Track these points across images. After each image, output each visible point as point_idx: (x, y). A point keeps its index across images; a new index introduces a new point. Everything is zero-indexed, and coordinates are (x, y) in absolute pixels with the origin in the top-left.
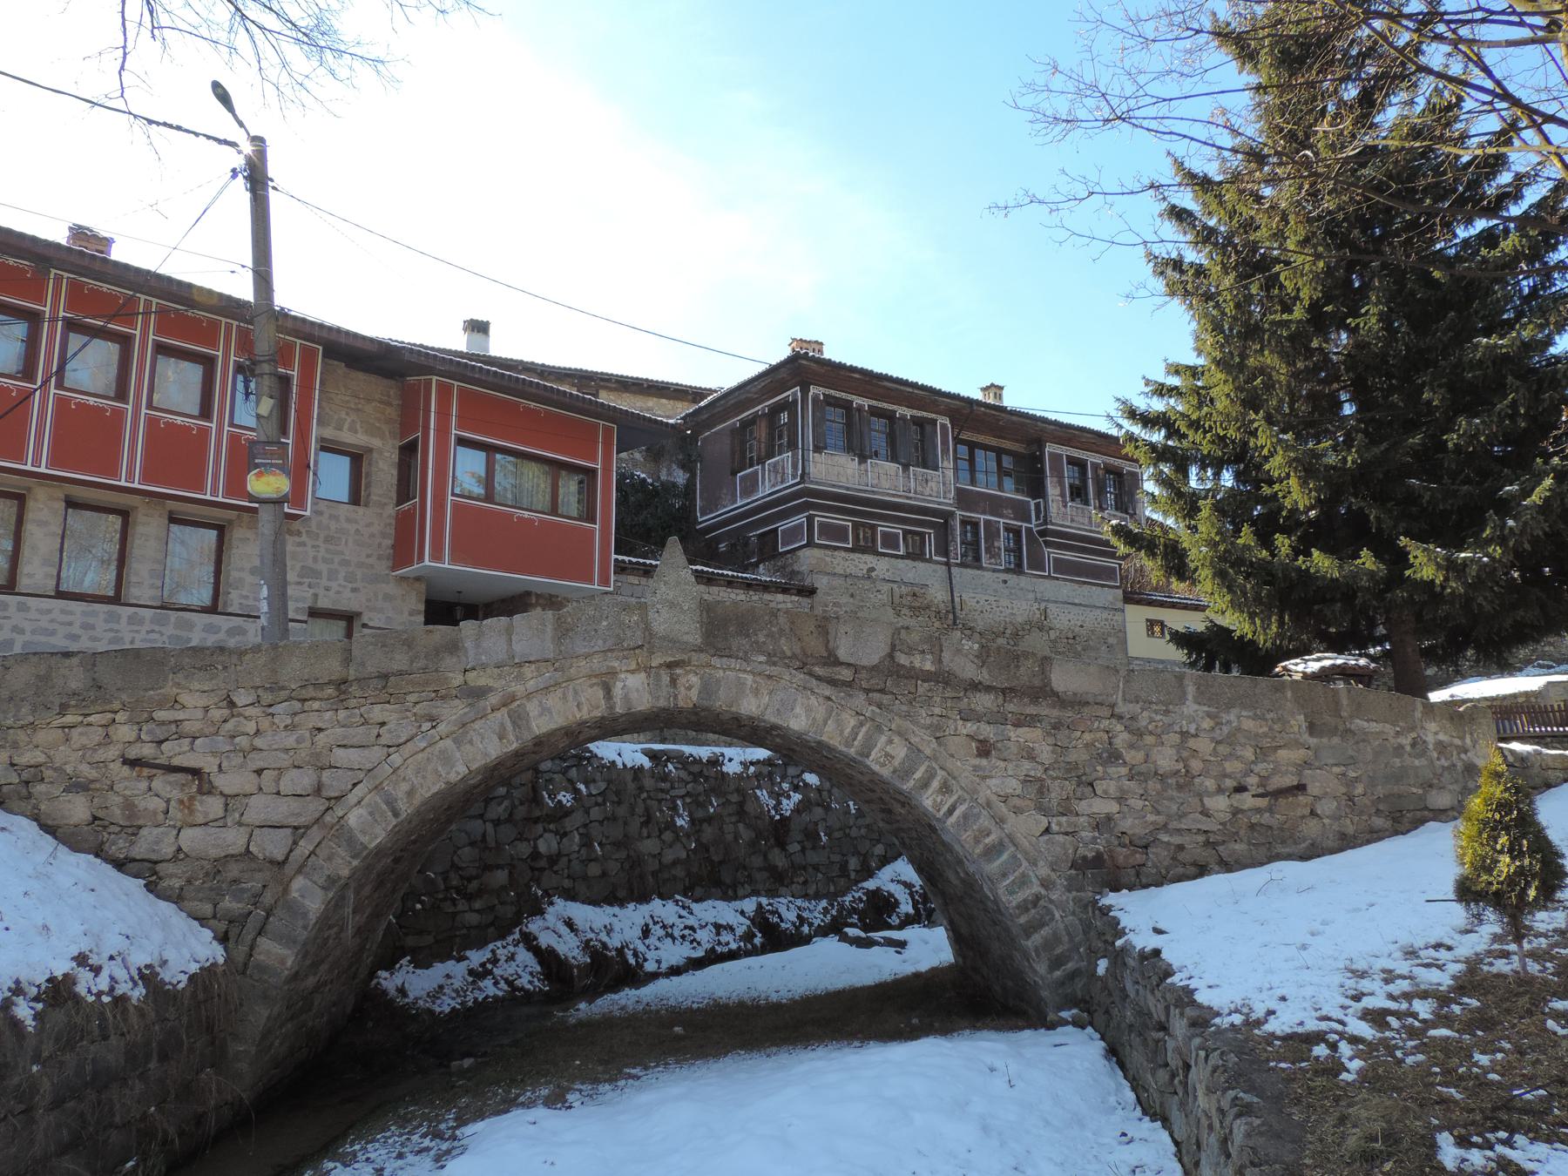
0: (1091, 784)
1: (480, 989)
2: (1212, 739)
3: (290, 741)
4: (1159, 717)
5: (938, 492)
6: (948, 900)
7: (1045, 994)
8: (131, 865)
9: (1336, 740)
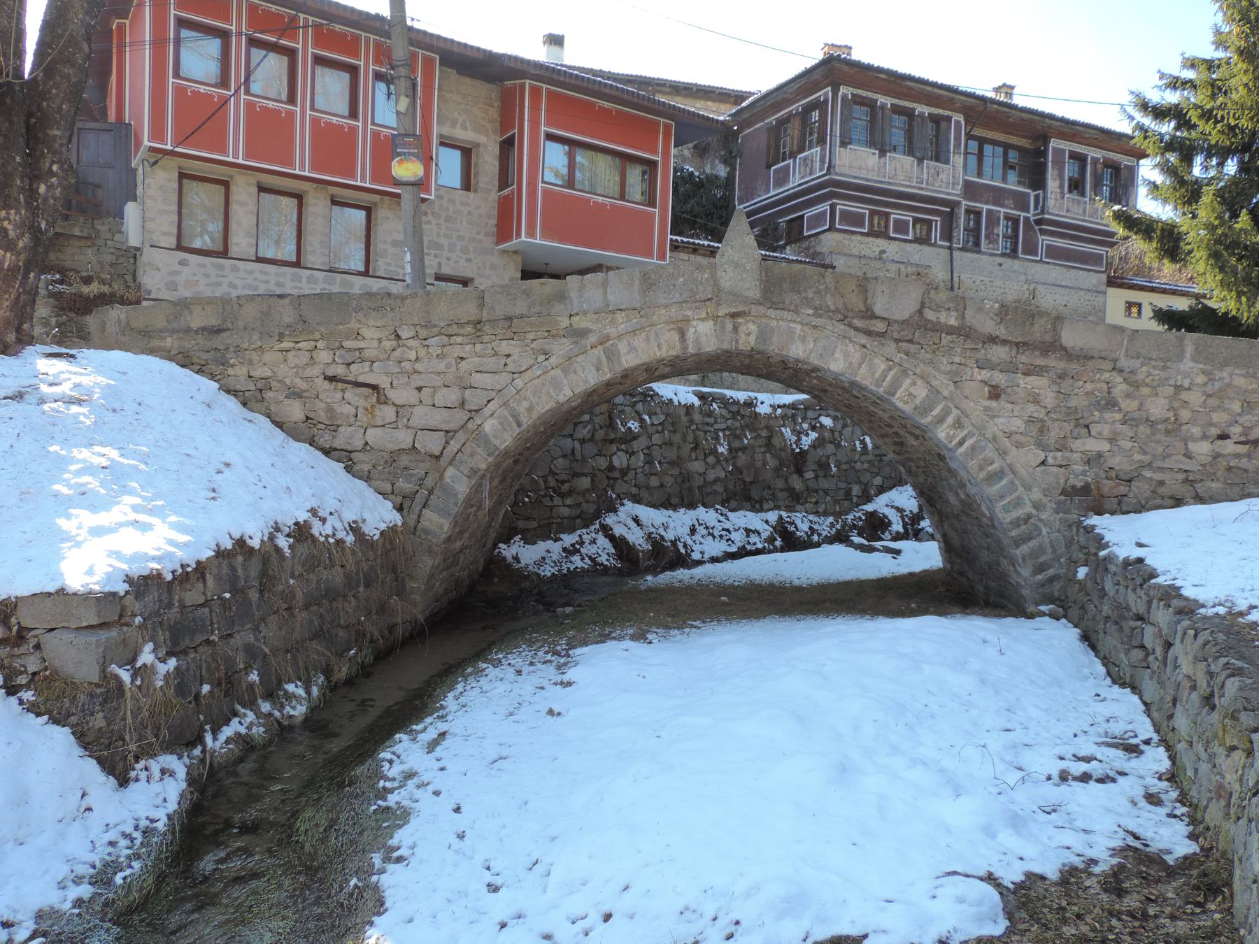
0: (1087, 427)
1: (571, 562)
2: (1204, 393)
3: (441, 366)
4: (1157, 372)
6: (941, 518)
7: (1026, 592)
8: (333, 453)
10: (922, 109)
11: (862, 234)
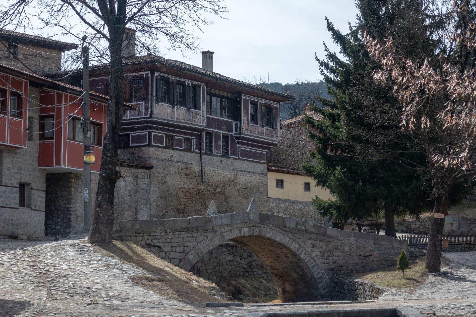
3: (178, 240)
5: (200, 121)
9: (378, 246)
10: (189, 82)
11: (163, 147)
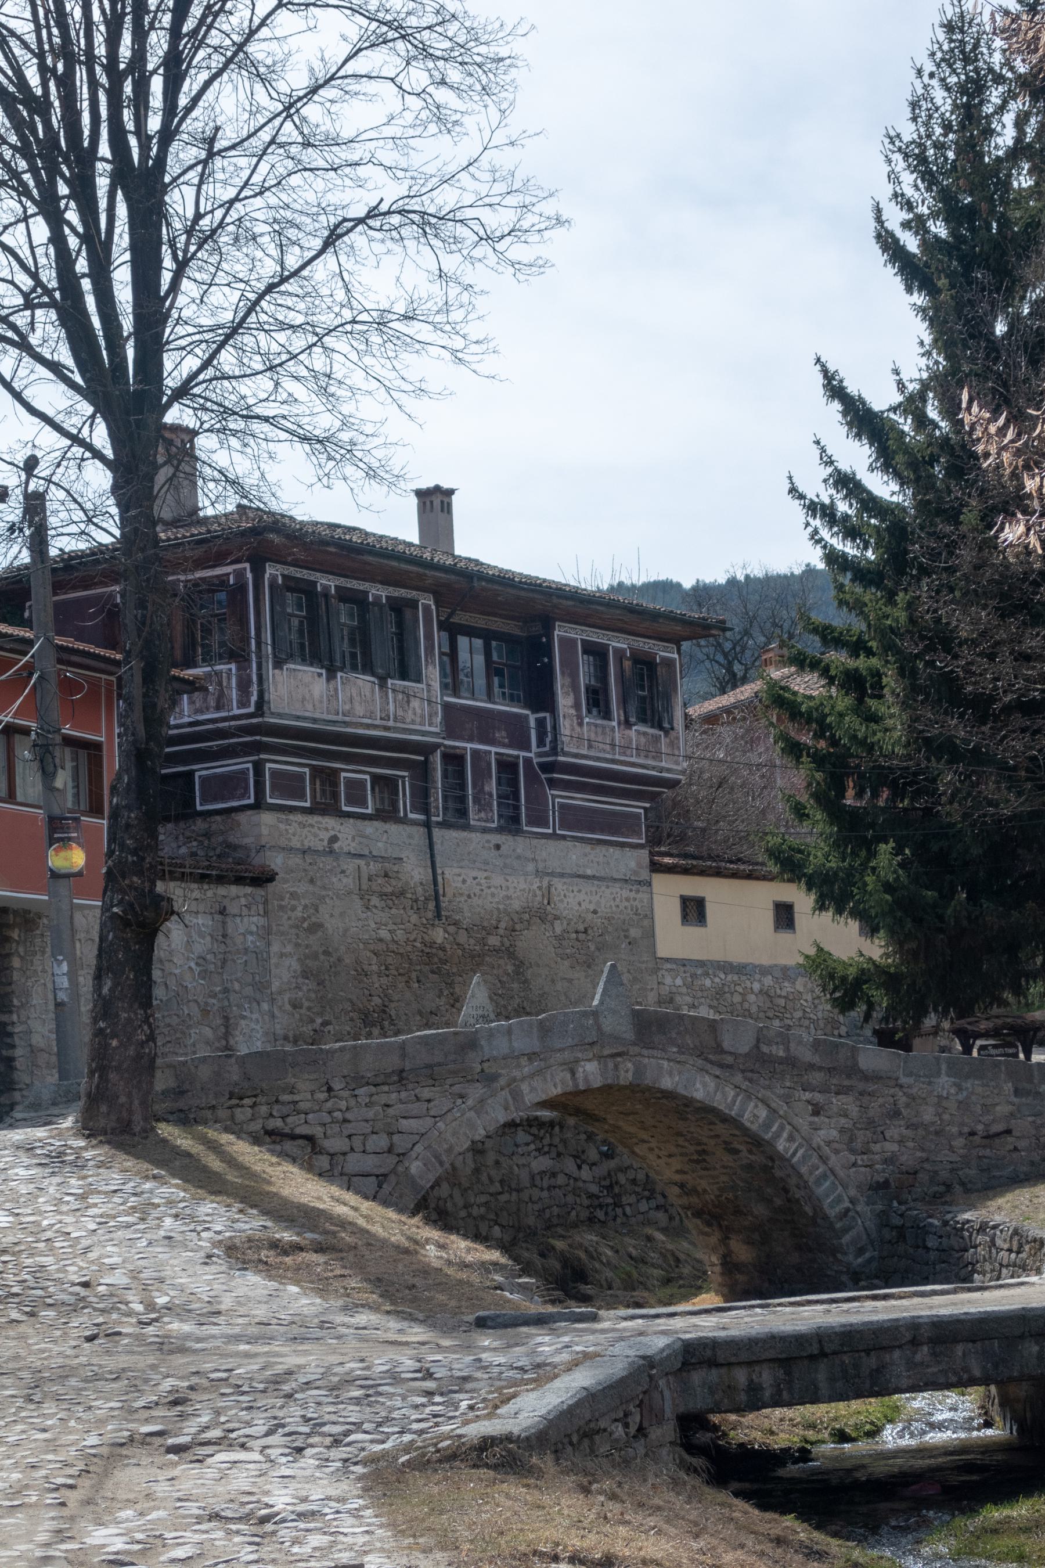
3: (371, 1114)
5: (422, 716)
9: (1029, 1100)
10: (377, 592)
